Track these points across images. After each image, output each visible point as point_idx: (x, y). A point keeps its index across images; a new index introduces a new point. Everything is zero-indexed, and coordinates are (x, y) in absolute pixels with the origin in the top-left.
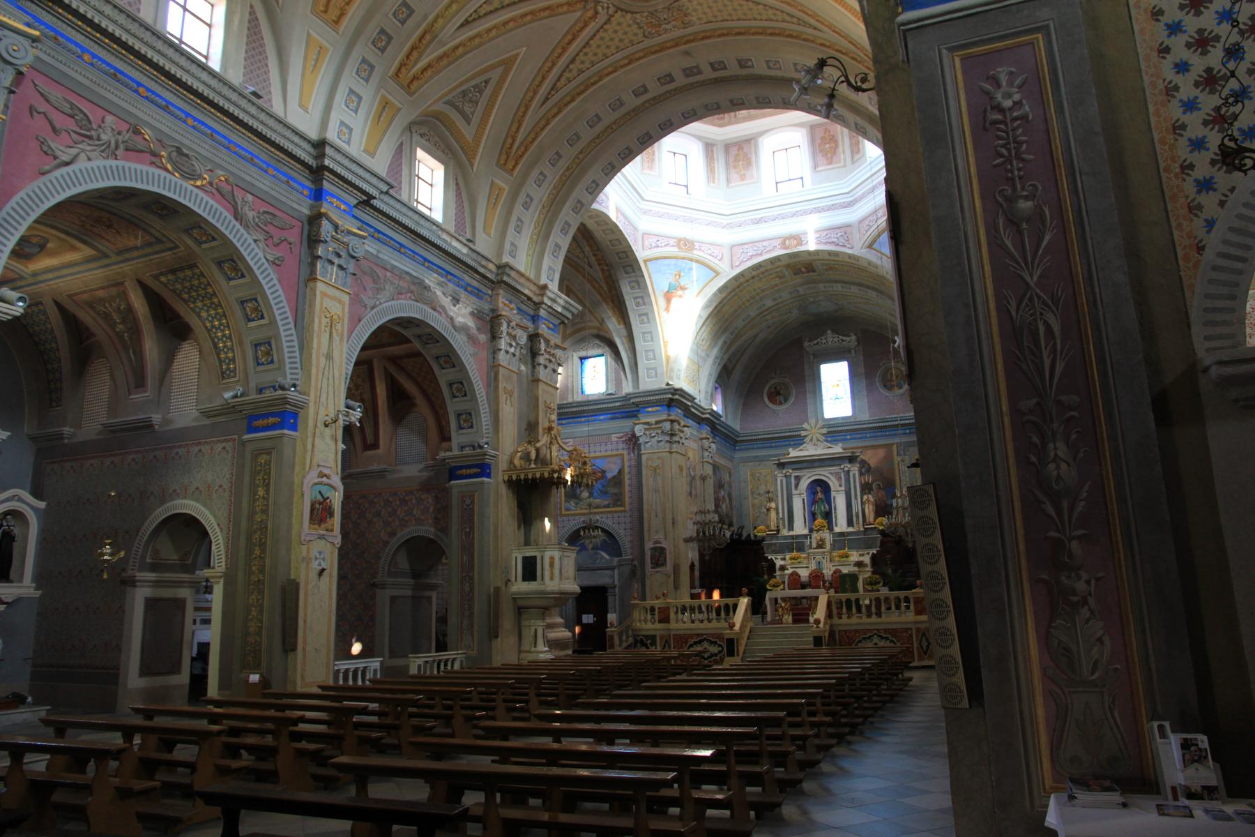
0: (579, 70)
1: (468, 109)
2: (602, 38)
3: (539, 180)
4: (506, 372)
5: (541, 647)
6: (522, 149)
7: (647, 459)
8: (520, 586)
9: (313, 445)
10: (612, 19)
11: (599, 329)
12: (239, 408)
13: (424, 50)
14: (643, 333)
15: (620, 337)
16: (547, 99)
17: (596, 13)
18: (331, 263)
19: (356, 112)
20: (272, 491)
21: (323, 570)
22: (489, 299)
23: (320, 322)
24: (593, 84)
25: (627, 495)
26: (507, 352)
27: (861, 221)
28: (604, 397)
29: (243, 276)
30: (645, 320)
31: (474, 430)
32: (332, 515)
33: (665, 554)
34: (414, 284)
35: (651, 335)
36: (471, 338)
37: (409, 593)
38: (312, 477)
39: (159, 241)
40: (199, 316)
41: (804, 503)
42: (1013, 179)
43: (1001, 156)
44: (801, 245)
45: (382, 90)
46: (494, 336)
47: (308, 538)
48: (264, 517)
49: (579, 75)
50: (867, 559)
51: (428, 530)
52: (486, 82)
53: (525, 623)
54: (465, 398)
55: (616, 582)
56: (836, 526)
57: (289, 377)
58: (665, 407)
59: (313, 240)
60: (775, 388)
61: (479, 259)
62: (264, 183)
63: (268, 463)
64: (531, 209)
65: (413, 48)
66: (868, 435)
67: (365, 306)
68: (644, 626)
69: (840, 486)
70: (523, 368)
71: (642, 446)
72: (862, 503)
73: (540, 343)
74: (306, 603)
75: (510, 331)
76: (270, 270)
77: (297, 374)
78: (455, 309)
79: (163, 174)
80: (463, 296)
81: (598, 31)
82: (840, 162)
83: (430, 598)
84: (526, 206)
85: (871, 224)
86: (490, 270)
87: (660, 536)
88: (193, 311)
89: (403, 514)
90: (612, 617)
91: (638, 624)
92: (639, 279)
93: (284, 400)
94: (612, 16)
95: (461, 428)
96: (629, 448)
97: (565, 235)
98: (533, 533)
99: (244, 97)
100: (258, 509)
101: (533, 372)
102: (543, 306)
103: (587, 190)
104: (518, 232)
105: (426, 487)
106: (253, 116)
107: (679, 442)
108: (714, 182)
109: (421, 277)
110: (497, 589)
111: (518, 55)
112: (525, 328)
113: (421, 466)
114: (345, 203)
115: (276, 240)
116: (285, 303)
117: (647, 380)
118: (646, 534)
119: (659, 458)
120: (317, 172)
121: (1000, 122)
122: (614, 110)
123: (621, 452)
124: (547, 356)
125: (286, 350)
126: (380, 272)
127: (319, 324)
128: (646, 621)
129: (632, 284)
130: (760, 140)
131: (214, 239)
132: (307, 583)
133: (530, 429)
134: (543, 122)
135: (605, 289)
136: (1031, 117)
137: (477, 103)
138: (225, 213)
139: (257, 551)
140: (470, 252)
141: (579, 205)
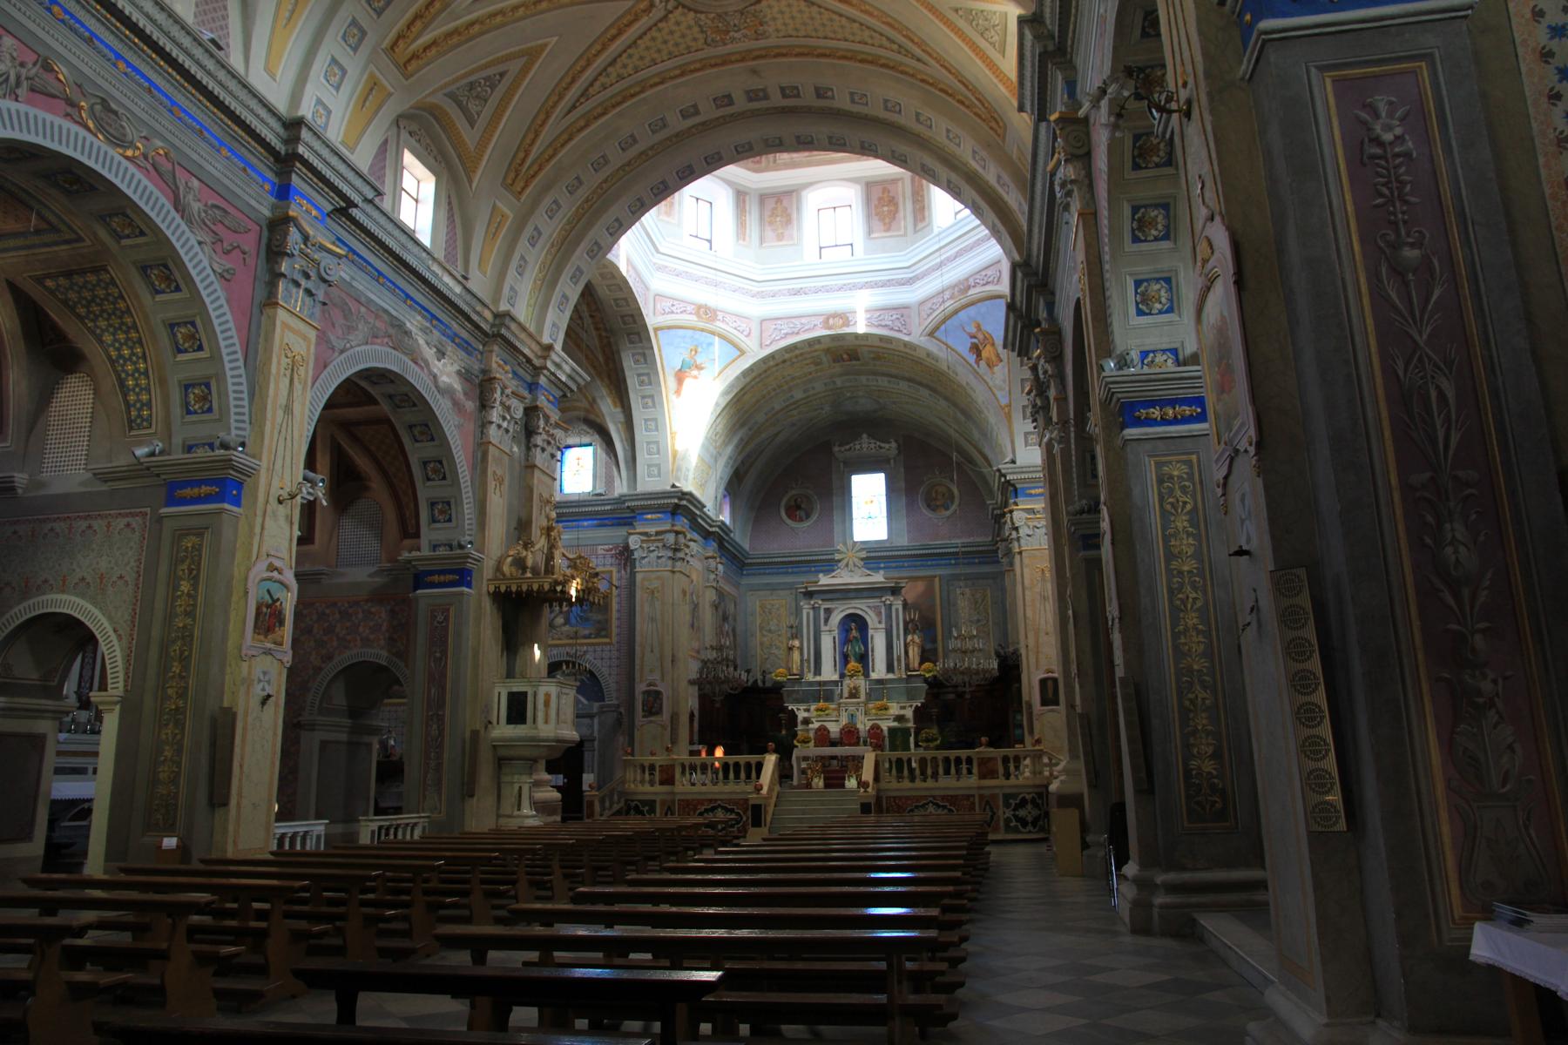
1: (473, 107)
2: (653, 39)
3: (552, 210)
4: (497, 452)
5: (526, 810)
6: (535, 168)
7: (643, 579)
8: (504, 731)
9: (263, 528)
11: (587, 411)
12: (156, 470)
13: (433, 19)
14: (646, 420)
15: (615, 424)
16: (574, 107)
18: (298, 285)
19: (338, 88)
20: (201, 588)
21: (269, 696)
22: (479, 357)
23: (279, 363)
24: (632, 96)
25: (615, 623)
26: (499, 426)
27: (922, 303)
28: (590, 498)
29: (178, 289)
30: (650, 404)
31: (453, 524)
32: (282, 623)
33: (661, 699)
34: (393, 326)
35: (656, 424)
36: (456, 403)
37: (344, 737)
38: (259, 570)
39: (54, 229)
40: (101, 341)
41: (834, 642)
42: (1396, 223)
43: (1381, 195)
44: (848, 326)
45: (371, 65)
46: (484, 405)
47: (251, 653)
48: (189, 621)
50: (909, 713)
51: (379, 654)
52: (502, 75)
53: (505, 779)
54: (443, 482)
55: (596, 734)
56: (873, 671)
57: (234, 432)
58: (669, 515)
59: (275, 252)
60: (796, 500)
61: (474, 302)
62: (217, 166)
63: (198, 549)
64: (538, 246)
65: (417, 17)
66: (906, 564)
67: (333, 349)
68: (641, 788)
69: (880, 622)
70: (515, 449)
71: (637, 563)
72: (906, 646)
73: (539, 419)
74: (243, 741)
75: (505, 399)
76: (217, 285)
77: (244, 429)
78: (440, 364)
79: (83, 132)
80: (449, 349)
81: (650, 29)
82: (899, 229)
83: (369, 745)
84: (533, 242)
85: (934, 307)
86: (486, 320)
87: (656, 676)
88: (93, 333)
89: (367, 631)
90: (588, 779)
91: (632, 786)
92: (646, 352)
93: (228, 463)
94: (671, 12)
95: (434, 521)
96: (619, 564)
97: (575, 284)
98: (519, 662)
99: (200, 44)
100: (179, 610)
101: (527, 456)
102: (545, 372)
103: (607, 229)
104: (520, 274)
105: (378, 596)
106: (209, 73)
107: (683, 559)
108: (744, 240)
109: (401, 318)
110: (475, 734)
111: (546, 45)
112: (521, 398)
113: (373, 569)
114: (317, 208)
115: (226, 246)
116: (233, 332)
117: (647, 479)
118: (637, 675)
119: (658, 578)
120: (285, 162)
121: (1380, 157)
122: (654, 132)
123: (608, 568)
124: (545, 437)
125: (232, 396)
126: (353, 305)
127: (278, 364)
128: (642, 782)
129: (637, 357)
130: (804, 193)
131: (142, 233)
132: (246, 714)
133: (522, 528)
134: (565, 136)
135: (601, 359)
136: (1415, 155)
137: (486, 101)
138: (163, 200)
139: (176, 668)
140: (464, 293)
141: (595, 248)
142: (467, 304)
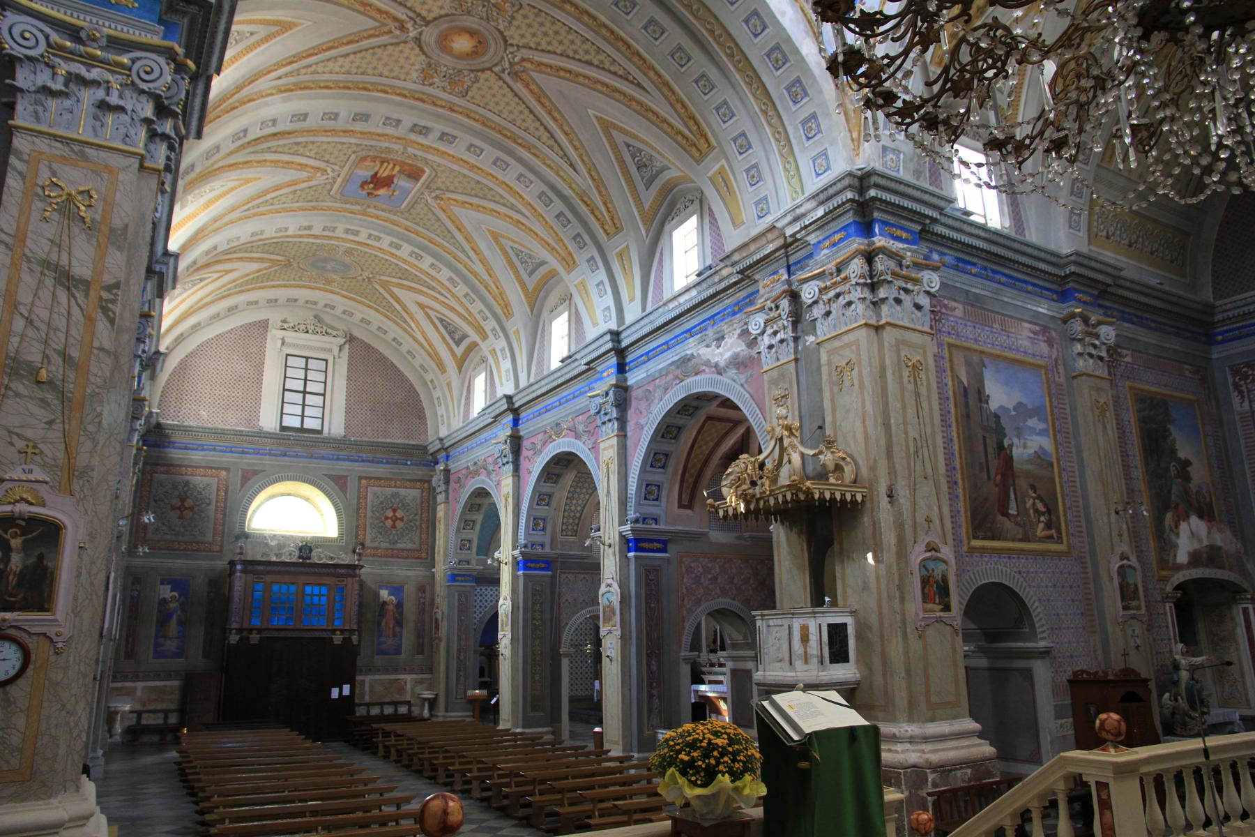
0: (598, 53)
2: (549, 43)
6: (691, 123)
10: (521, 44)
16: (639, 85)
17: (523, 60)
24: (612, 32)
49: (604, 52)
52: (628, 146)
81: (543, 51)
94: (518, 46)
103: (756, 36)
109: (683, 354)
111: (596, 117)
134: (665, 90)
140: (699, 288)
142: (709, 287)
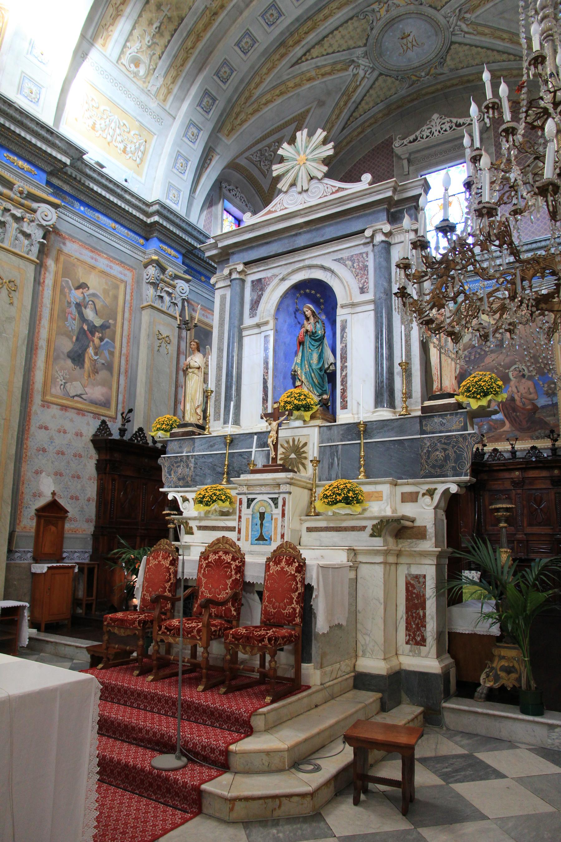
56: (344, 407)
